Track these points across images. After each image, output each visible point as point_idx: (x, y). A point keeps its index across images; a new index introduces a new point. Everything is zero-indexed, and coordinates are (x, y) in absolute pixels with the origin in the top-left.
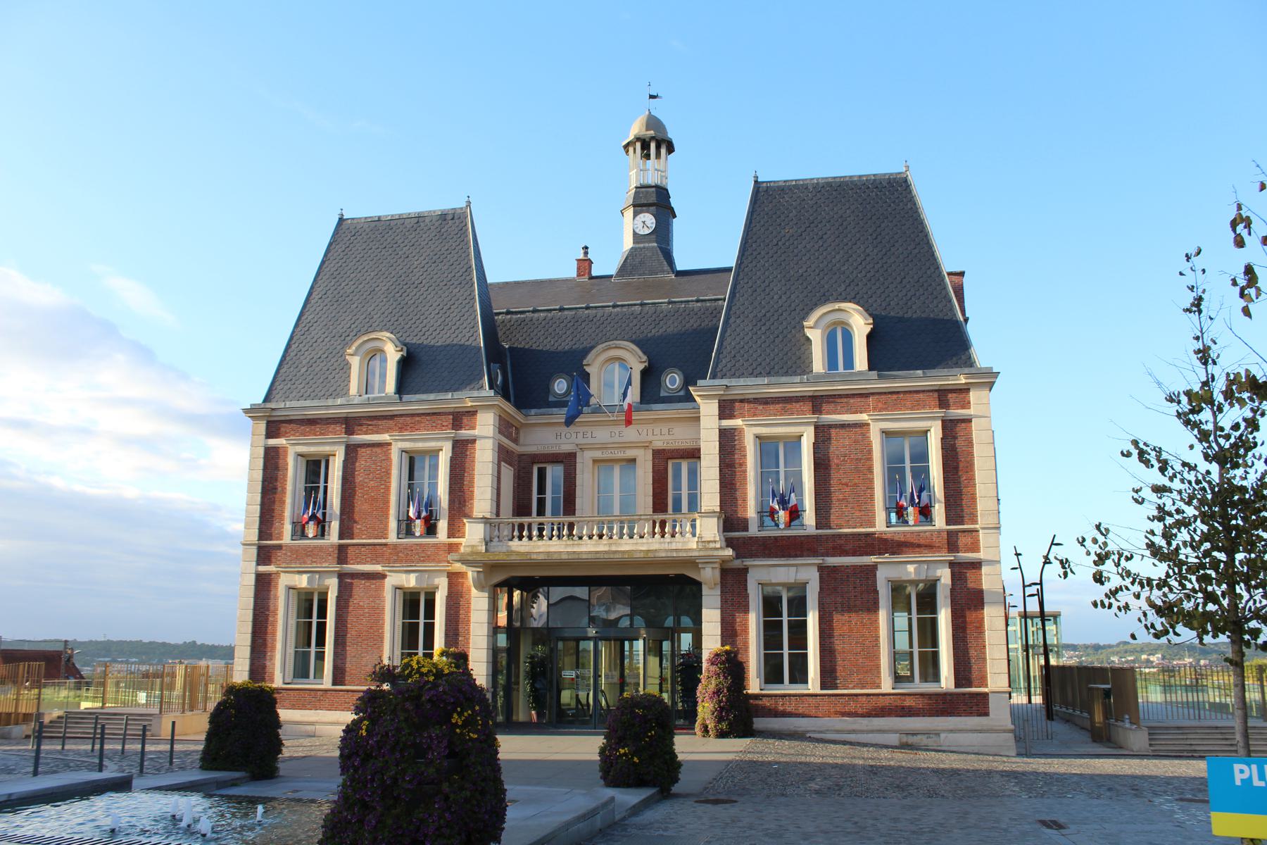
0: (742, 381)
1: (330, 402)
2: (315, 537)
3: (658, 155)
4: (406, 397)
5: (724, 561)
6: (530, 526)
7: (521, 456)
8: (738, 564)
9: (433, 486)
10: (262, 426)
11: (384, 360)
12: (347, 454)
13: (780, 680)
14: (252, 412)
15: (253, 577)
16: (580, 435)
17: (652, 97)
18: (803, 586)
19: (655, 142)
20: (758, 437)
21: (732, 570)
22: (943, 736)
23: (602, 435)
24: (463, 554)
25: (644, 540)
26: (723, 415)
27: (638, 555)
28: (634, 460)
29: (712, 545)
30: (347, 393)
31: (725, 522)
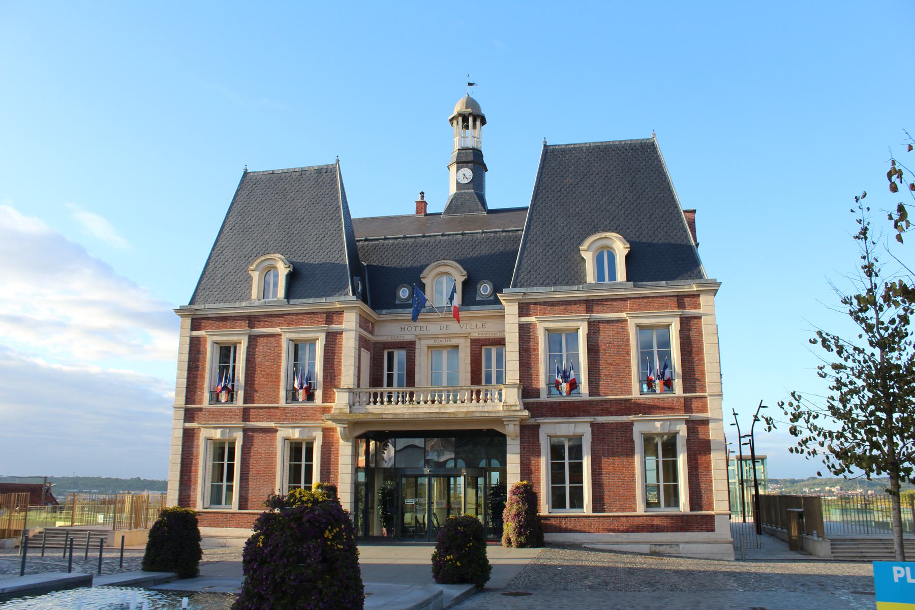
0: (535, 290)
1: (237, 304)
2: (226, 402)
3: (474, 126)
4: (292, 301)
6: (382, 394)
7: (375, 343)
8: (532, 421)
9: (312, 365)
10: (188, 322)
12: (249, 342)
14: (181, 311)
15: (181, 431)
16: (418, 329)
17: (470, 84)
18: (580, 438)
19: (472, 117)
20: (547, 330)
21: (528, 426)
22: (681, 546)
23: (434, 328)
24: (333, 415)
25: (464, 404)
26: (521, 314)
27: (460, 415)
28: (457, 347)
29: (514, 408)
30: (249, 298)
31: (523, 391)
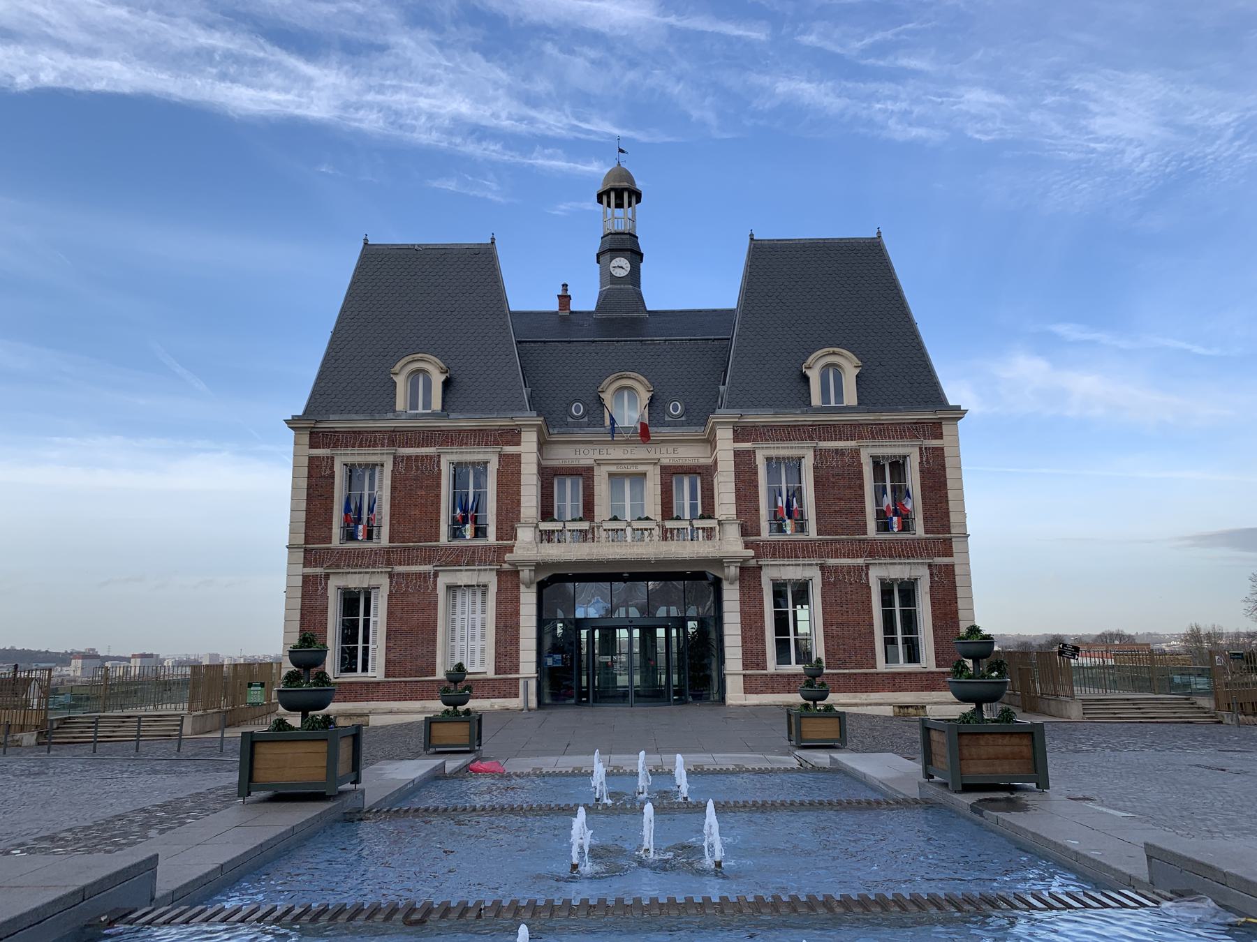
1: (345, 416)
3: (630, 205)
5: (746, 560)
8: (753, 562)
14: (293, 423)
16: (597, 452)
19: (621, 193)
20: (769, 459)
21: (748, 569)
23: (616, 453)
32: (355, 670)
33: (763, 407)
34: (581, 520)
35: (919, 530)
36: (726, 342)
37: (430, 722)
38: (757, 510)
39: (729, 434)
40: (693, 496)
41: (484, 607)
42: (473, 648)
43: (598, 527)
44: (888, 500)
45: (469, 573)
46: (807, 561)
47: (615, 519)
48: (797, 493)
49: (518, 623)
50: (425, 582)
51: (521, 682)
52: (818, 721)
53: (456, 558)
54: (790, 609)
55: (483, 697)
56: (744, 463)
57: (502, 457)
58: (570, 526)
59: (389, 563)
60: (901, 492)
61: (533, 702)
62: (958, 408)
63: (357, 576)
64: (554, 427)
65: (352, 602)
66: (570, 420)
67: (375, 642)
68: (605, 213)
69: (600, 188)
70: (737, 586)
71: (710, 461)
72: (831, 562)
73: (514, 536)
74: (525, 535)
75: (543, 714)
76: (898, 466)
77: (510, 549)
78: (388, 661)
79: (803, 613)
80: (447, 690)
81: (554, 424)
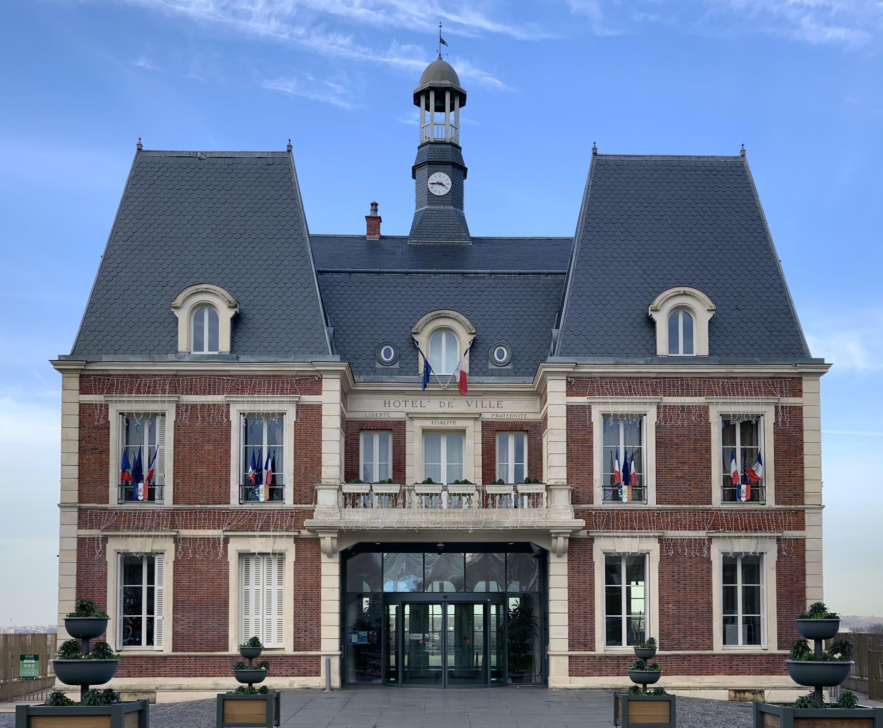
5: (576, 531)
8: (583, 534)
11: (214, 319)
13: (619, 642)
16: (409, 404)
20: (606, 416)
23: (432, 405)
28: (463, 431)
32: (139, 643)
33: (602, 355)
34: (390, 482)
35: (770, 499)
36: (561, 277)
37: (223, 700)
38: (591, 474)
39: (562, 385)
40: (519, 457)
41: (280, 578)
42: (269, 622)
43: (410, 491)
44: (736, 467)
45: (264, 539)
46: (643, 533)
47: (429, 482)
48: (636, 456)
49: (319, 596)
50: (215, 548)
51: (323, 660)
52: (648, 704)
53: (248, 523)
54: (624, 586)
55: (281, 675)
56: (578, 421)
57: (301, 409)
58: (378, 489)
59: (173, 526)
60: (752, 456)
61: (336, 682)
62: (820, 362)
63: (139, 539)
64: (361, 374)
65: (134, 568)
66: (378, 366)
67: (160, 613)
68: (422, 117)
69: (417, 86)
70: (565, 559)
71: (539, 417)
72: (671, 534)
73: (314, 500)
74: (327, 499)
75: (346, 694)
76: (750, 427)
77: (310, 514)
78: (175, 634)
79: (637, 590)
80: (240, 666)
81: (358, 372)
